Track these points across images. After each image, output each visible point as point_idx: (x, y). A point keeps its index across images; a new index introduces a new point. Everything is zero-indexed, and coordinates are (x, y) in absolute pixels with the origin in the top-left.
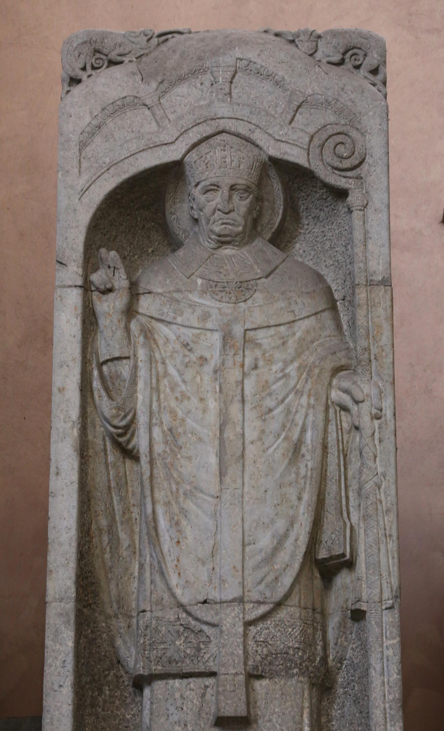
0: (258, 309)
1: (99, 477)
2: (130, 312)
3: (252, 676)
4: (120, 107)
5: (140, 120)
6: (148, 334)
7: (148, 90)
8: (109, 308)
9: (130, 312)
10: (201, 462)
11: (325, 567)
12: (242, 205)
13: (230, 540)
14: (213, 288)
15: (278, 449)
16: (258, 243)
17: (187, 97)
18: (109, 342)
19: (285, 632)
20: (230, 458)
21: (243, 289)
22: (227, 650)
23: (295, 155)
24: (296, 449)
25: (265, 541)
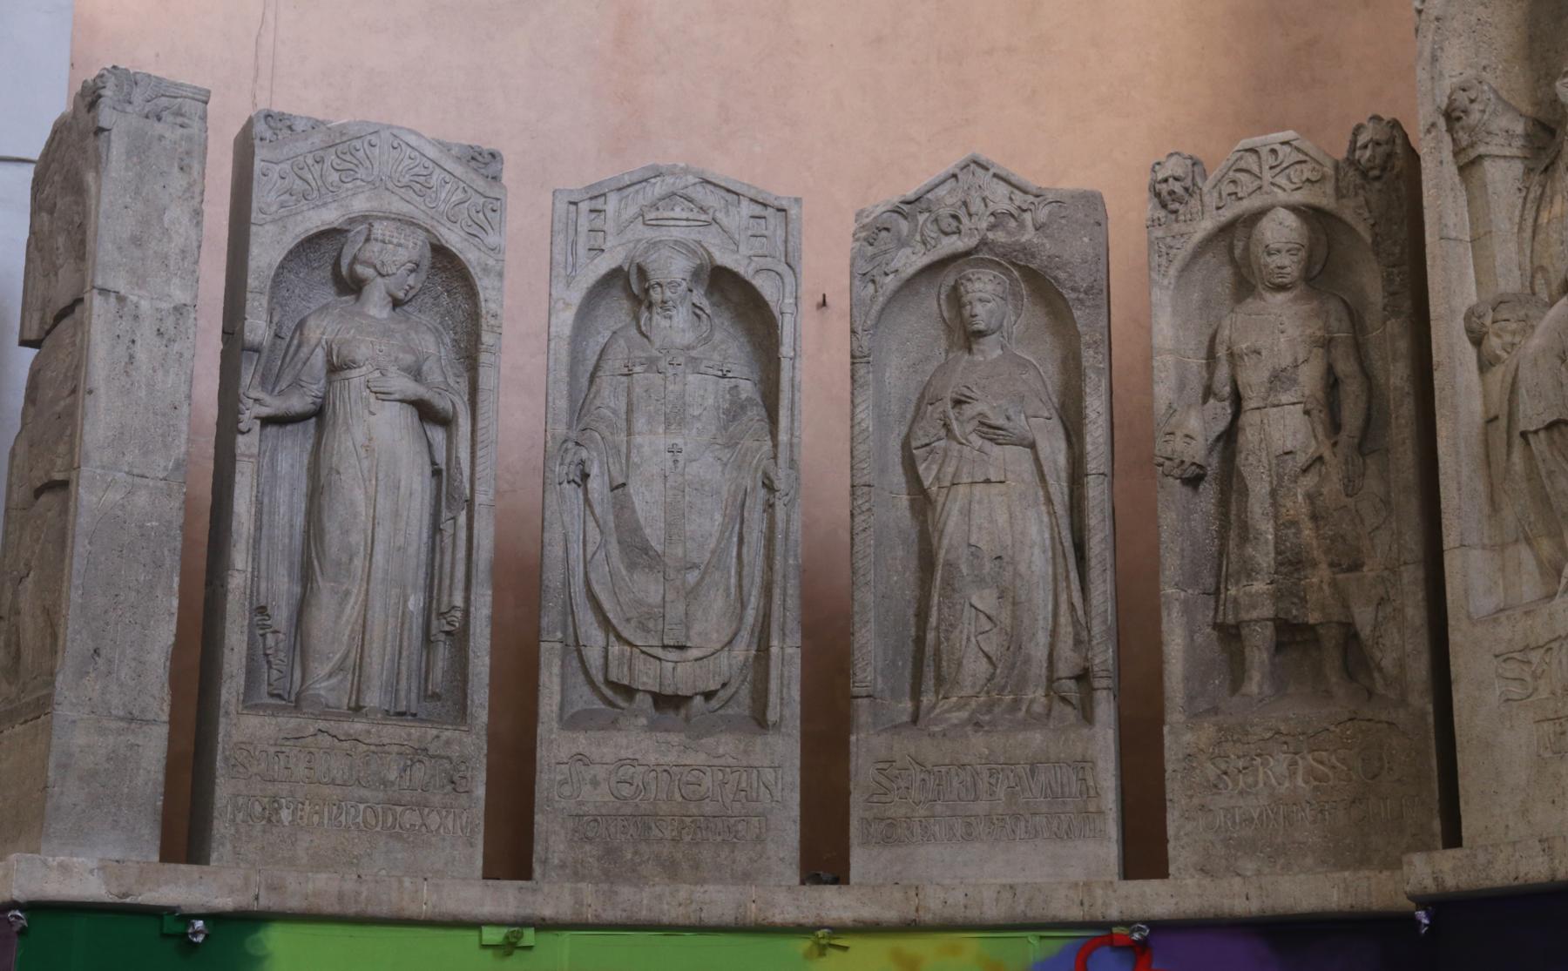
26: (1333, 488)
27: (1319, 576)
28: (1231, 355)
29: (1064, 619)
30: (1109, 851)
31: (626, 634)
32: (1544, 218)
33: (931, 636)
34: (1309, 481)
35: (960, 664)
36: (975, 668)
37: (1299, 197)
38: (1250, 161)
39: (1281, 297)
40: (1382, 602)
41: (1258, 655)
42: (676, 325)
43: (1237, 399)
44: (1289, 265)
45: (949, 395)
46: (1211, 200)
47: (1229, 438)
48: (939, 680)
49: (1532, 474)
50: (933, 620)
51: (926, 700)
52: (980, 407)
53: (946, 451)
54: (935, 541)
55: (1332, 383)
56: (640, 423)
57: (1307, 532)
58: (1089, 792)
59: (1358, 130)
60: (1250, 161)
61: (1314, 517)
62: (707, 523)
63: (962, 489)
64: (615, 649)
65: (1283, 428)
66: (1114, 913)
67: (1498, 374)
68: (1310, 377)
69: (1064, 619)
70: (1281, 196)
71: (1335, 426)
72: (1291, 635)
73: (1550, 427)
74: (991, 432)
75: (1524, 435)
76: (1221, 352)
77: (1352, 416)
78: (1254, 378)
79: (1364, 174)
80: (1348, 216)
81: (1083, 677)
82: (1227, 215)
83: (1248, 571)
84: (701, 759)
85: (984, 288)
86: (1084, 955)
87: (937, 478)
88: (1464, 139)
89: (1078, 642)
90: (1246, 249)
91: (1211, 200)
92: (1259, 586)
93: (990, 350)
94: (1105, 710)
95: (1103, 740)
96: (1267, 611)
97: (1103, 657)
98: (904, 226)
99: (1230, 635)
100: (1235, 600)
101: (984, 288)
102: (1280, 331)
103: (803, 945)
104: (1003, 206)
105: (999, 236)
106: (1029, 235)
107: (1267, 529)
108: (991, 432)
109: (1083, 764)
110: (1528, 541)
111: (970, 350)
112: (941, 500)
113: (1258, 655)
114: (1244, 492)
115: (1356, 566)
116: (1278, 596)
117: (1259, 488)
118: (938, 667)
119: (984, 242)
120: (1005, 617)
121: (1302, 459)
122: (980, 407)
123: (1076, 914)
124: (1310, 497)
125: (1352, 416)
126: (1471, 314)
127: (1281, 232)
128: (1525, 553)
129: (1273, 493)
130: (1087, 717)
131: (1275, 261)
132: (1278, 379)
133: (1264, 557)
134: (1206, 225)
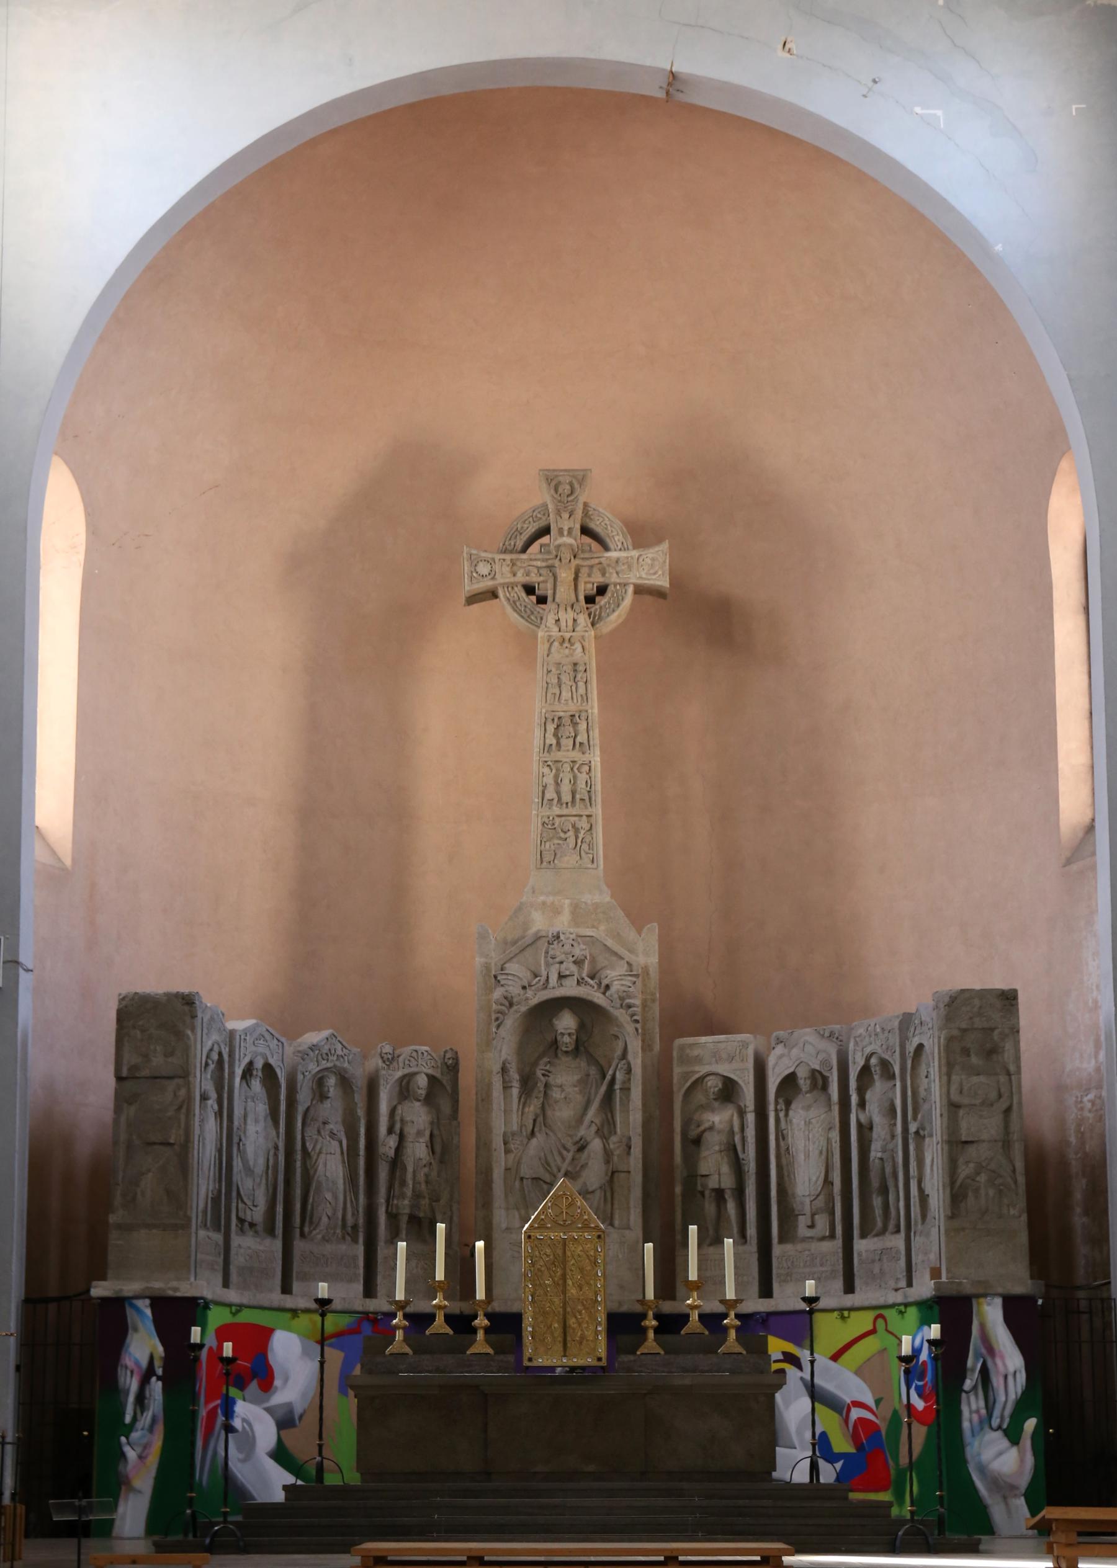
0: (812, 1113)
1: (784, 1161)
2: (787, 1115)
3: (813, 1215)
4: (781, 1057)
5: (785, 1060)
6: (791, 1121)
7: (786, 1051)
8: (782, 1114)
9: (787, 1115)
10: (801, 1157)
11: (828, 1182)
12: (808, 1082)
13: (807, 1179)
14: (803, 1108)
15: (817, 1152)
16: (815, 1092)
17: (795, 1051)
18: (783, 1125)
19: (820, 1202)
20: (807, 1156)
21: (808, 1108)
22: (807, 1209)
23: (818, 1068)
24: (821, 1152)
25: (814, 1179)
26: (434, 1174)
27: (425, 1202)
28: (402, 1120)
29: (349, 1205)
30: (359, 1287)
31: (245, 1200)
32: (526, 1110)
33: (309, 1207)
34: (426, 1170)
35: (320, 1219)
36: (325, 1219)
37: (430, 1071)
38: (414, 1054)
39: (418, 1104)
40: (445, 1213)
41: (403, 1226)
42: (256, 1085)
43: (402, 1137)
44: (422, 1092)
45: (321, 1120)
46: (401, 1065)
47: (399, 1149)
48: (311, 1223)
49: (522, 1189)
50: (311, 1200)
51: (306, 1229)
52: (331, 1126)
53: (317, 1141)
54: (312, 1172)
55: (432, 1135)
56: (249, 1121)
57: (423, 1186)
58: (356, 1266)
59: (446, 1052)
60: (414, 1054)
61: (427, 1182)
62: (261, 1161)
63: (323, 1156)
64: (241, 1205)
65: (418, 1150)
66: (371, 1309)
67: (511, 1156)
68: (427, 1133)
69: (349, 1205)
70: (425, 1070)
71: (433, 1153)
72: (413, 1219)
73: (533, 1179)
74: (332, 1135)
75: (522, 1179)
76: (398, 1118)
77: (438, 1148)
78: (411, 1131)
79: (448, 1067)
80: (444, 1082)
81: (355, 1227)
82: (407, 1071)
83: (403, 1196)
84: (261, 1248)
85: (332, 1081)
86: (360, 1321)
87: (314, 1148)
88: (507, 1079)
89: (353, 1214)
90: (408, 1083)
91: (401, 1065)
92: (406, 1202)
93: (327, 1104)
94: (361, 1240)
95: (360, 1250)
96: (407, 1211)
97: (361, 1221)
98: (311, 1053)
99: (393, 1217)
100: (397, 1206)
101: (332, 1081)
102: (417, 1116)
103: (289, 1315)
104: (339, 1052)
105: (338, 1064)
106: (346, 1065)
107: (410, 1182)
108: (332, 1135)
109: (355, 1258)
110: (518, 1209)
111: (322, 1102)
112: (315, 1157)
113: (403, 1226)
114: (405, 1169)
115: (438, 1200)
116: (412, 1207)
117: (410, 1169)
118: (311, 1218)
119: (335, 1066)
120: (333, 1204)
121: (424, 1162)
122: (331, 1126)
123: (360, 1309)
124: (426, 1175)
125: (438, 1148)
126: (505, 1134)
127: (422, 1081)
128: (516, 1213)
129: (414, 1172)
130: (355, 1241)
131: (420, 1091)
132: (419, 1133)
133: (409, 1192)
134: (399, 1074)
